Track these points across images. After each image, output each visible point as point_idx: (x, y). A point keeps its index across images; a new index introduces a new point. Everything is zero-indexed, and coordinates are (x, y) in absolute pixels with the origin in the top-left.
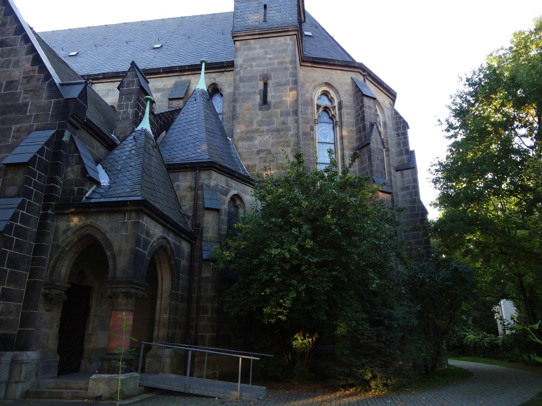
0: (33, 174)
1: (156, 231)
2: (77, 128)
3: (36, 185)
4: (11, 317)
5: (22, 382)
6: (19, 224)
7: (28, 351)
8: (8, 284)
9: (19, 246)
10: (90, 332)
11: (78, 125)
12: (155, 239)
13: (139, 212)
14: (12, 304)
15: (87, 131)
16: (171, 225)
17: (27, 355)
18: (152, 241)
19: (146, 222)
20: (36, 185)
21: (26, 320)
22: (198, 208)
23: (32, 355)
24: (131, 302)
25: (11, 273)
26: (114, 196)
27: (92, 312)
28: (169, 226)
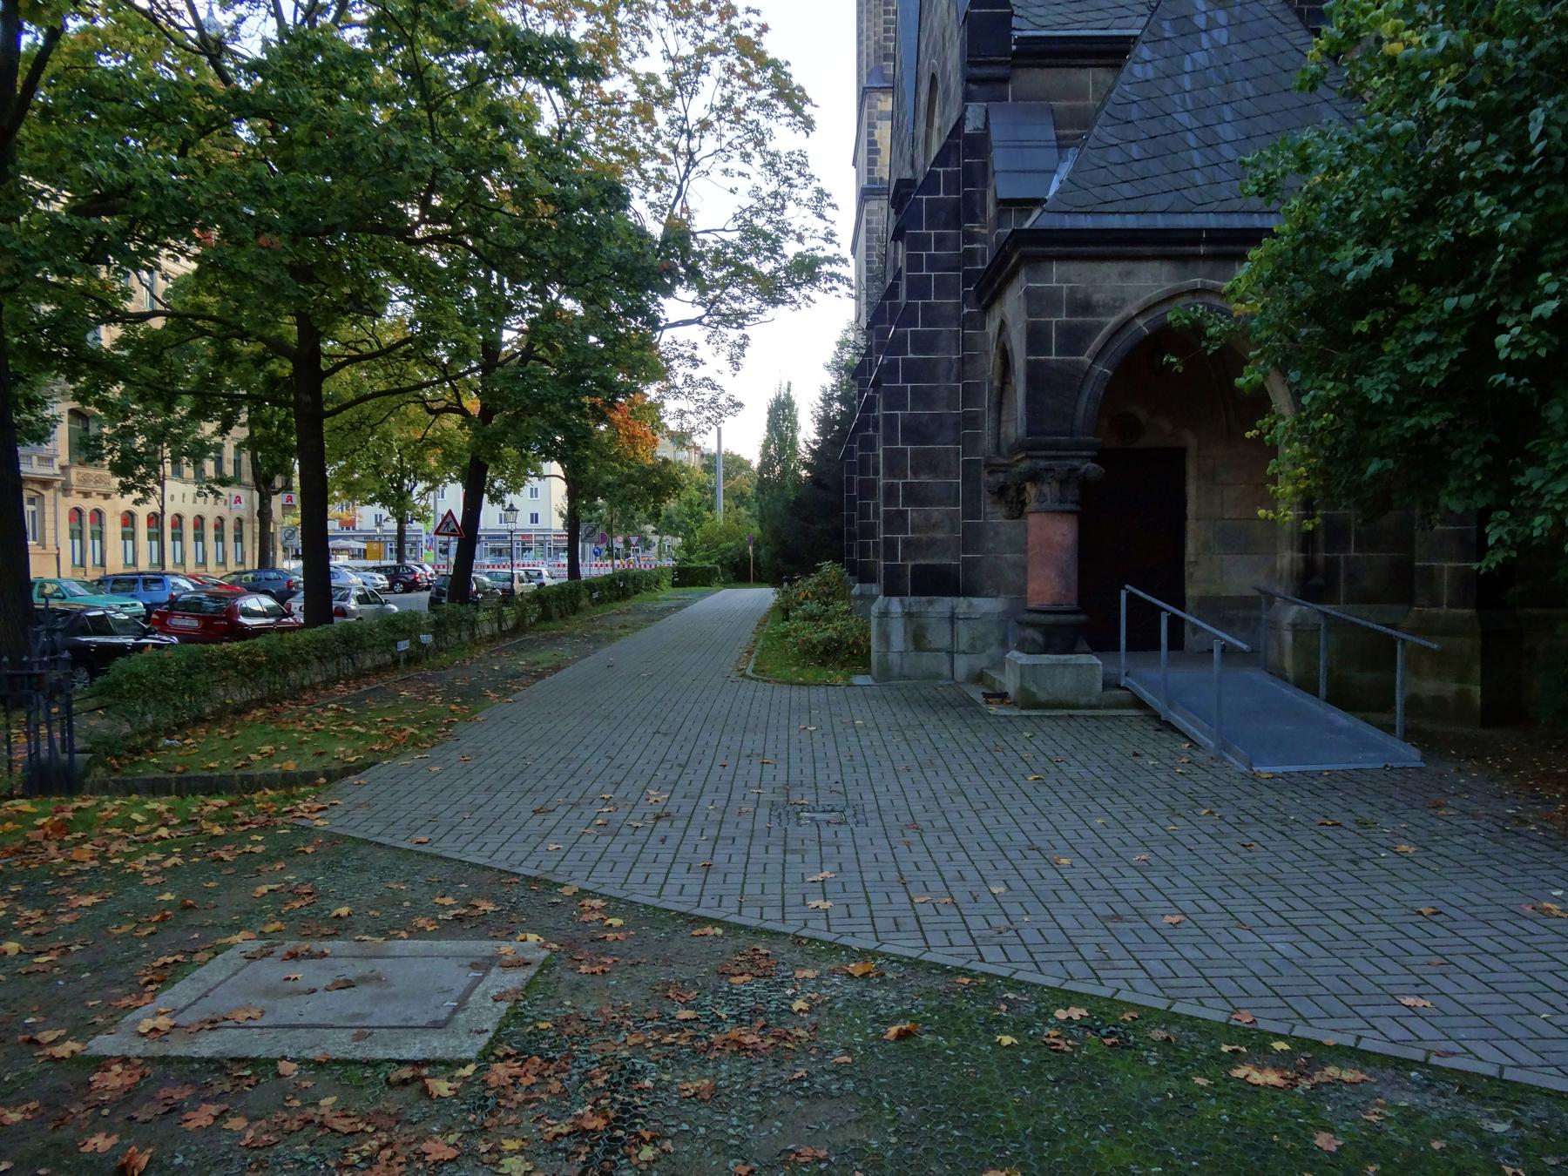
0: (923, 242)
1: (1139, 287)
2: (1005, 80)
3: (933, 263)
4: (940, 535)
5: (964, 653)
6: (910, 356)
7: (976, 594)
8: (915, 474)
9: (922, 398)
10: (1193, 559)
11: (998, 71)
12: (1131, 309)
13: (1035, 261)
14: (937, 512)
15: (1041, 66)
16: (1208, 242)
17: (970, 605)
18: (1112, 321)
19: (1062, 277)
20: (933, 263)
21: (972, 538)
22: (272, 416)
23: (988, 605)
24: (1050, 489)
25: (915, 454)
26: (1123, 207)
27: (1191, 508)
28: (1202, 250)
